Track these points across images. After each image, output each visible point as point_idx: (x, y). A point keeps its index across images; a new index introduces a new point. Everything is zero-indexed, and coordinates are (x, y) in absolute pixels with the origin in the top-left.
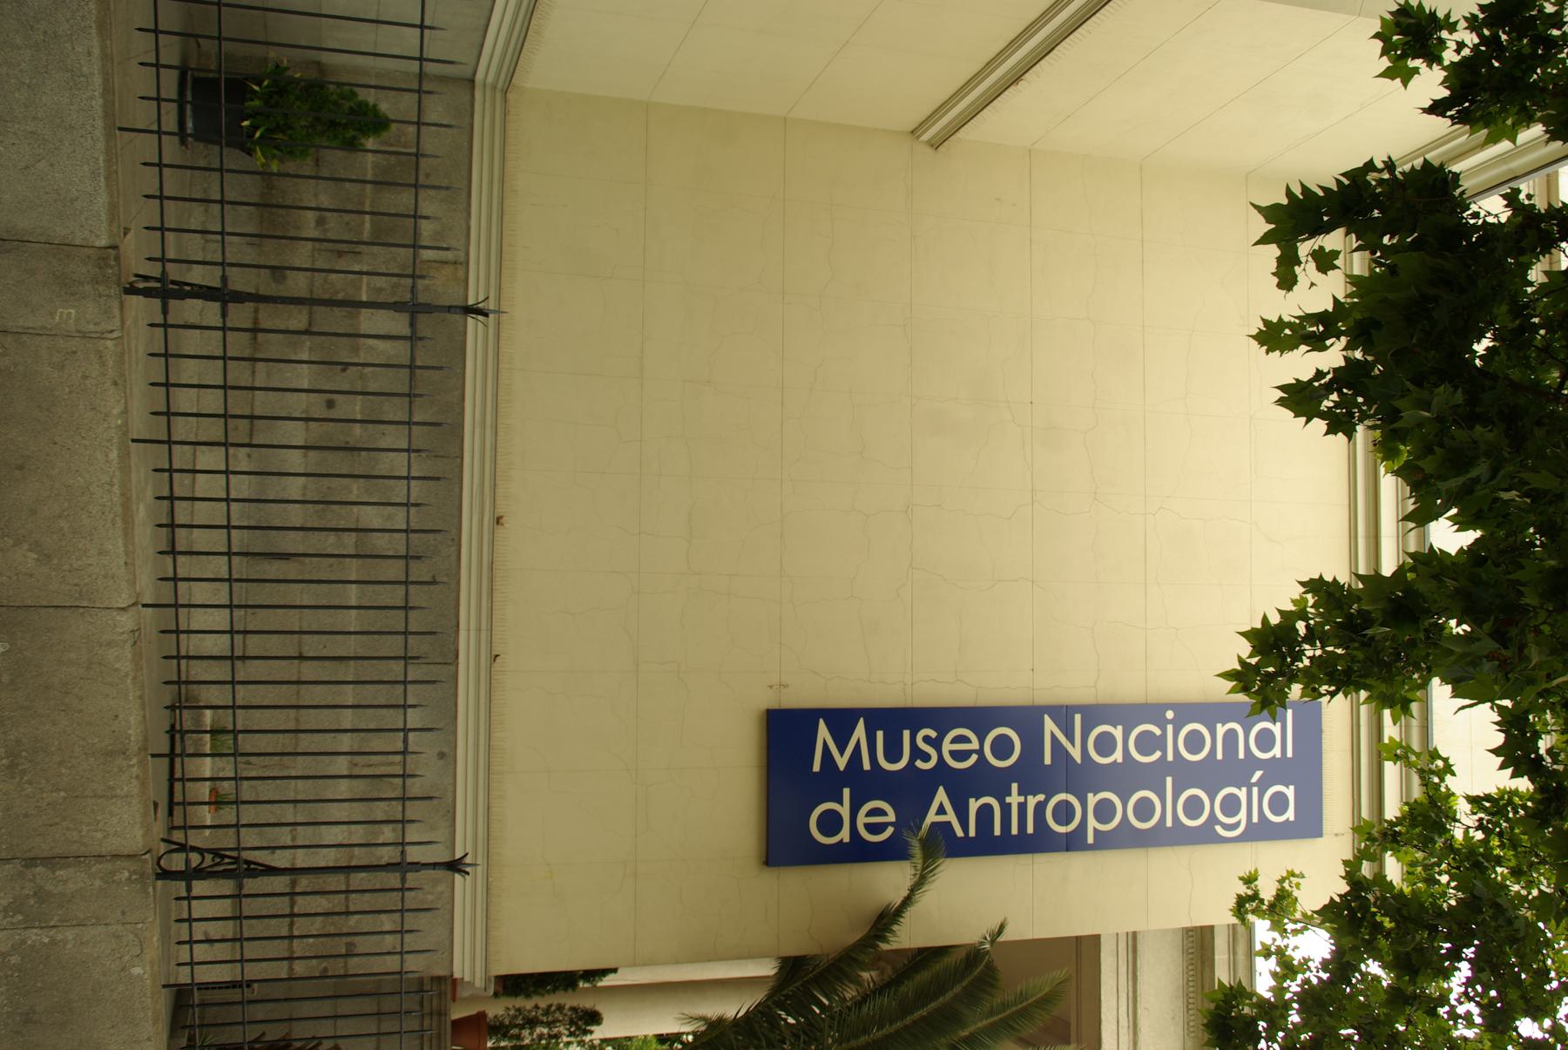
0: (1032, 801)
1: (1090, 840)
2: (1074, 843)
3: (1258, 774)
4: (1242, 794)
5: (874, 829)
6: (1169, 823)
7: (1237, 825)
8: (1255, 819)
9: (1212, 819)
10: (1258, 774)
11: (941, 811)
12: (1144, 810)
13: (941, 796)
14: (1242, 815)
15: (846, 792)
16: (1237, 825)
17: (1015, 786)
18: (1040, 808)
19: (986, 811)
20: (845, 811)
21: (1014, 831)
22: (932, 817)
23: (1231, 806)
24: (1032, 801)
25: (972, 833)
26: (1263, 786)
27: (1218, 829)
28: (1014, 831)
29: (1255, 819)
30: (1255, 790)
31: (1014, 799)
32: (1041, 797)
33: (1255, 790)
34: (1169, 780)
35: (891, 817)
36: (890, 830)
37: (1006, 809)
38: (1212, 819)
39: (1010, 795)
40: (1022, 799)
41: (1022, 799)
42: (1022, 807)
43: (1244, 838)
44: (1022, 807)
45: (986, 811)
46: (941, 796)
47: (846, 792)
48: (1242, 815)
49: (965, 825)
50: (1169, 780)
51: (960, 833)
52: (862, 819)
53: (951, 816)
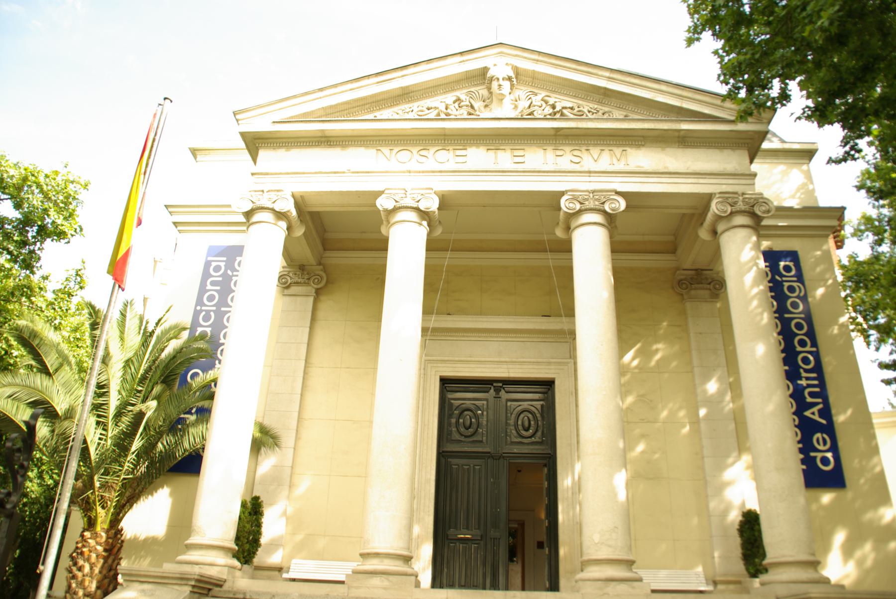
0: (804, 374)
1: (814, 349)
2: (817, 356)
3: (777, 278)
4: (786, 284)
5: (825, 443)
6: (803, 316)
7: (799, 287)
8: (795, 279)
9: (798, 297)
10: (777, 278)
11: (813, 413)
12: (799, 326)
13: (807, 413)
14: (795, 284)
15: (812, 454)
16: (799, 287)
17: (799, 382)
18: (806, 371)
19: (812, 395)
20: (819, 455)
21: (816, 382)
22: (816, 417)
23: (792, 289)
24: (804, 374)
25: (819, 400)
26: (781, 276)
27: (802, 294)
28: (816, 382)
29: (795, 279)
30: (784, 279)
31: (803, 382)
32: (802, 371)
33: (784, 279)
34: (786, 316)
35: (819, 435)
36: (825, 436)
37: (809, 386)
38: (797, 297)
39: (802, 385)
40: (804, 379)
41: (804, 379)
42: (807, 379)
43: (803, 283)
44: (807, 379)
45: (812, 395)
46: (807, 413)
47: (812, 454)
48: (795, 284)
49: (817, 404)
50: (786, 316)
51: (821, 406)
52: (821, 447)
53: (815, 409)
